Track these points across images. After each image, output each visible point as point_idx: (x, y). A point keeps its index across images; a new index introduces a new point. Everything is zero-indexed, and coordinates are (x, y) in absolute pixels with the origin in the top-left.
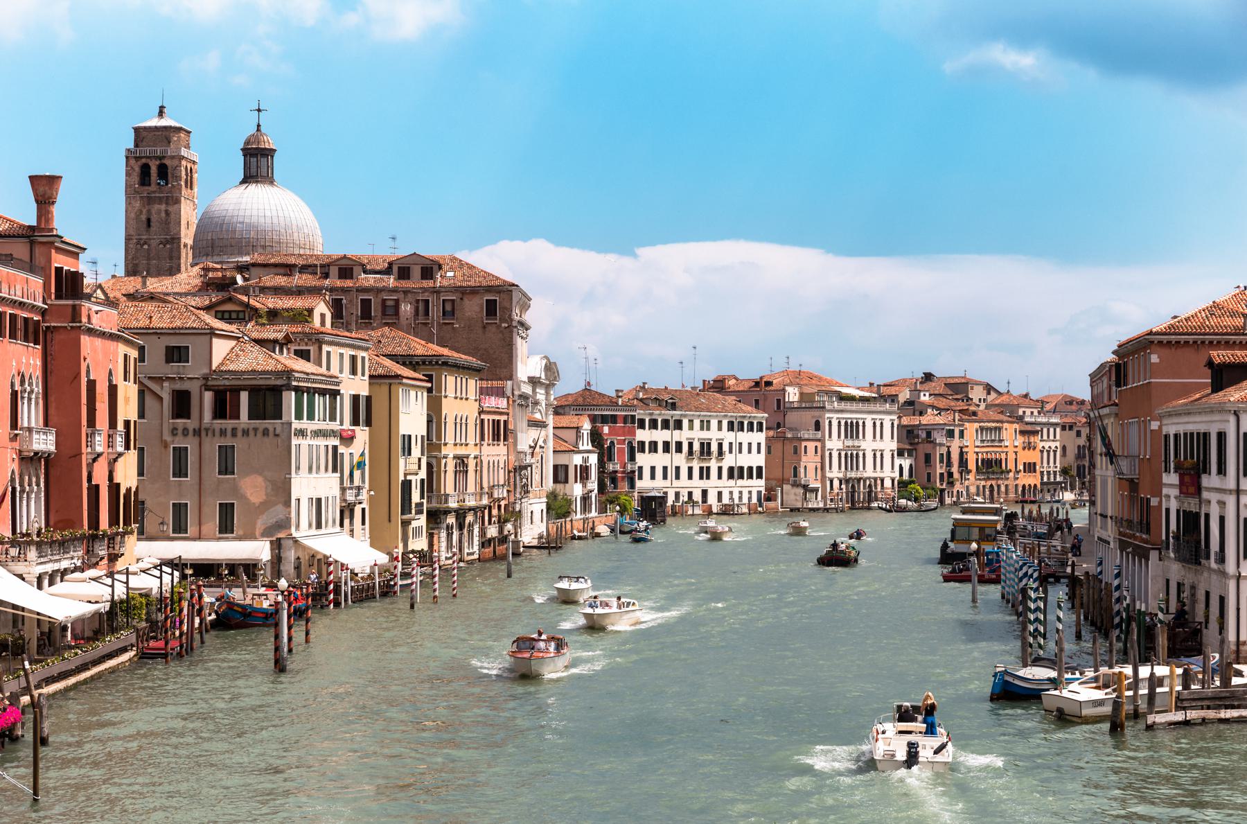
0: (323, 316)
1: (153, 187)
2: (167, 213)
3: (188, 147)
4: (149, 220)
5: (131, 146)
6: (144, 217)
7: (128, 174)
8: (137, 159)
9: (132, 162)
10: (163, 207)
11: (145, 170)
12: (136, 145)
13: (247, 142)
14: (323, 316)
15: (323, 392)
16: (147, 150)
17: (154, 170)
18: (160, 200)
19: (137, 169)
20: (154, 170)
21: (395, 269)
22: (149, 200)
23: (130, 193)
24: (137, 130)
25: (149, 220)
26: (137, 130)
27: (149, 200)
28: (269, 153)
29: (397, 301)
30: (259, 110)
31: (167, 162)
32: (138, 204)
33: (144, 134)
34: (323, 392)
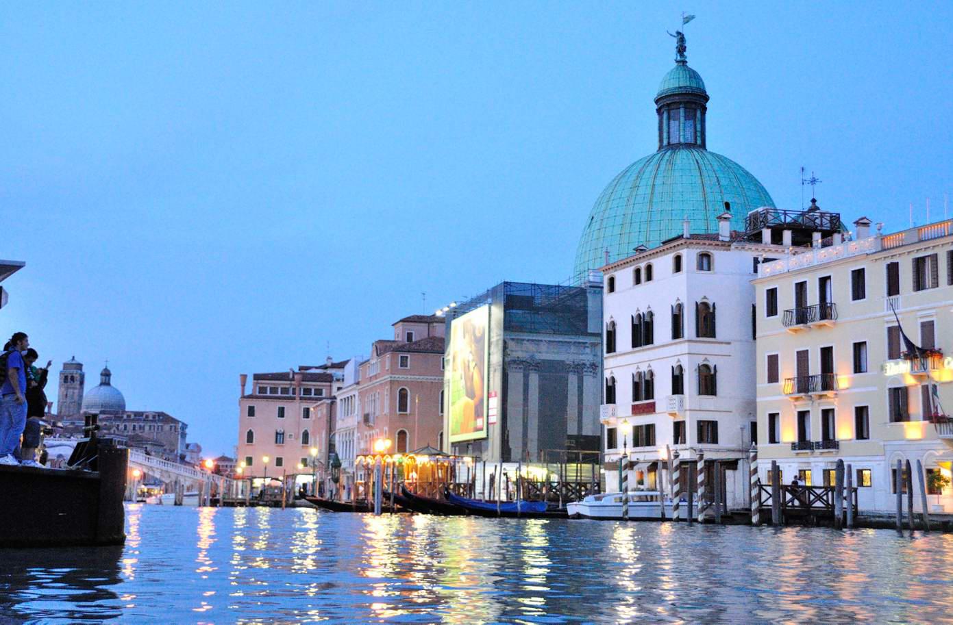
1: (69, 384)
2: (74, 393)
3: (81, 369)
4: (66, 395)
6: (65, 394)
7: (60, 379)
11: (66, 378)
12: (64, 369)
16: (68, 372)
17: (69, 378)
18: (71, 388)
20: (69, 378)
21: (144, 416)
22: (67, 388)
23: (61, 386)
25: (66, 395)
27: (67, 388)
30: (107, 361)
31: (74, 375)
32: (63, 389)
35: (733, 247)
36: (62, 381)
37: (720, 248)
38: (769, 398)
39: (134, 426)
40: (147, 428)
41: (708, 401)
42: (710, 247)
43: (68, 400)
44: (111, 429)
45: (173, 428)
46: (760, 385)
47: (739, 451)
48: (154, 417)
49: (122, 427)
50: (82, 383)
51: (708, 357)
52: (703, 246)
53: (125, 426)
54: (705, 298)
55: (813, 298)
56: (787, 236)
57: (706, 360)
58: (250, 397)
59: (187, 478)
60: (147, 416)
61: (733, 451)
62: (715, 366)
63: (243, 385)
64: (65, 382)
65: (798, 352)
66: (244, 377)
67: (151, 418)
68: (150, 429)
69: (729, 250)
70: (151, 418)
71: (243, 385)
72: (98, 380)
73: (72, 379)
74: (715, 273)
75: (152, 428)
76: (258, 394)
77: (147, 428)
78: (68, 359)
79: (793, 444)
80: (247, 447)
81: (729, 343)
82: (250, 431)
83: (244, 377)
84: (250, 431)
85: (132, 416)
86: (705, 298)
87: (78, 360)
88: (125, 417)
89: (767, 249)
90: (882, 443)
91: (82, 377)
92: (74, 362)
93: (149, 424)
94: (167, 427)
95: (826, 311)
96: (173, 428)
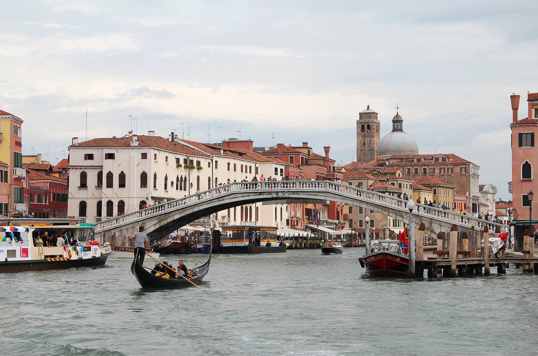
0: (399, 174)
1: (366, 132)
2: (370, 140)
3: (377, 119)
5: (359, 119)
6: (363, 142)
8: (360, 123)
9: (359, 124)
10: (369, 139)
11: (363, 127)
13: (394, 118)
14: (399, 174)
15: (396, 193)
16: (363, 121)
17: (366, 127)
19: (361, 127)
20: (366, 127)
22: (365, 137)
23: (358, 135)
24: (360, 114)
26: (360, 114)
27: (365, 137)
28: (401, 121)
29: (434, 168)
33: (362, 115)
34: (396, 193)
36: (360, 130)
39: (425, 169)
40: (437, 171)
43: (367, 148)
44: (395, 173)
45: (463, 170)
48: (444, 159)
49: (413, 171)
50: (378, 130)
53: (416, 170)
58: (526, 122)
59: (442, 224)
60: (437, 159)
63: (515, 108)
64: (362, 131)
66: (515, 99)
67: (440, 161)
68: (440, 172)
70: (440, 161)
71: (515, 108)
72: (390, 126)
73: (369, 127)
75: (442, 170)
76: (533, 118)
77: (437, 171)
78: (363, 109)
80: (524, 184)
82: (527, 162)
83: (515, 99)
84: (527, 162)
85: (423, 160)
87: (373, 109)
88: (415, 161)
91: (378, 126)
92: (369, 111)
93: (438, 167)
94: (457, 169)
96: (463, 170)
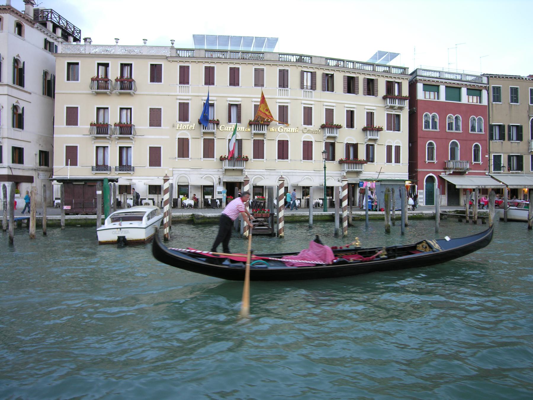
35: (36, 26)
37: (29, 23)
38: (66, 136)
41: (18, 133)
42: (23, 20)
46: (57, 126)
47: (35, 170)
51: (19, 101)
52: (19, 17)
54: (18, 56)
55: (114, 73)
56: (59, 32)
57: (17, 102)
61: (32, 169)
62: (23, 108)
65: (68, 108)
69: (33, 27)
74: (24, 40)
79: (92, 167)
81: (30, 93)
86: (18, 56)
89: (49, 34)
90: (171, 169)
95: (126, 84)
